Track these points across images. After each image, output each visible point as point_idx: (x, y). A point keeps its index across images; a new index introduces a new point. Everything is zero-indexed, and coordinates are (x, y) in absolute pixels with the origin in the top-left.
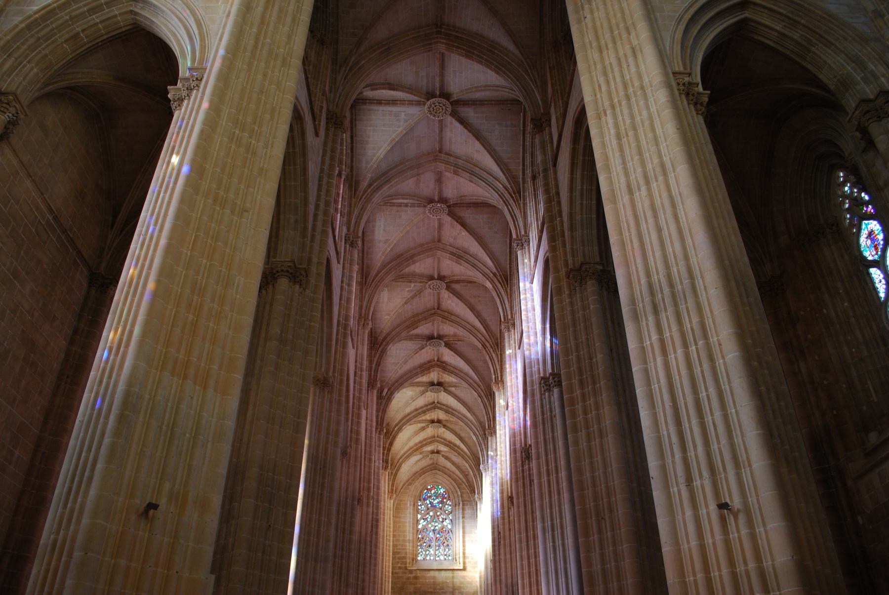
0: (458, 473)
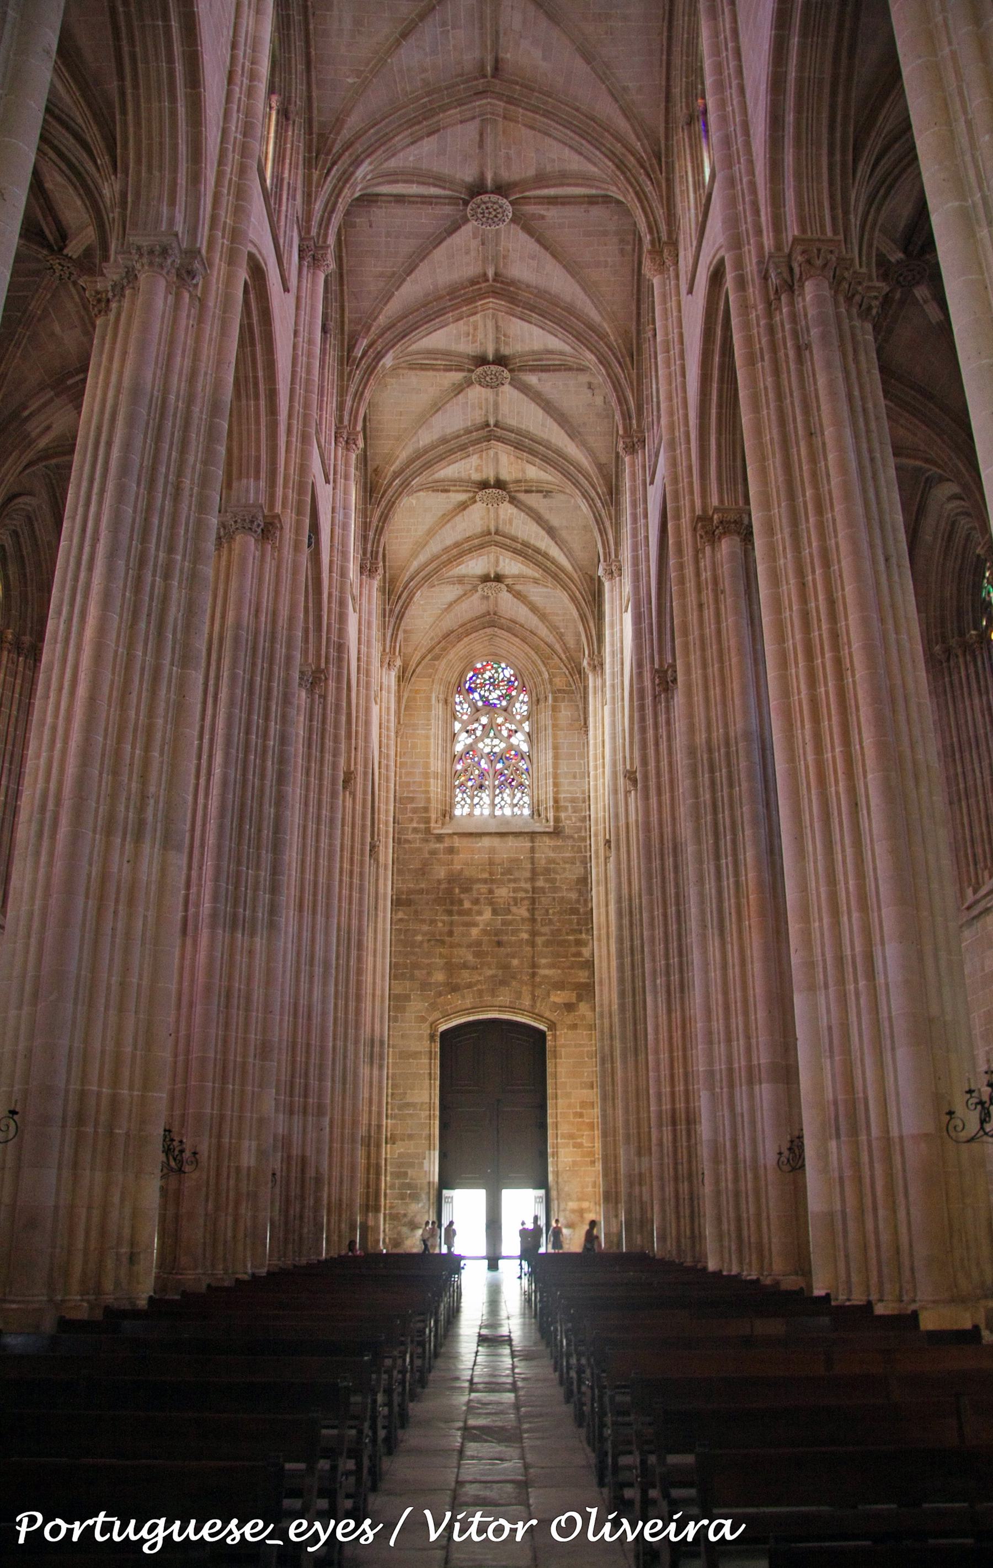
0: (543, 631)
